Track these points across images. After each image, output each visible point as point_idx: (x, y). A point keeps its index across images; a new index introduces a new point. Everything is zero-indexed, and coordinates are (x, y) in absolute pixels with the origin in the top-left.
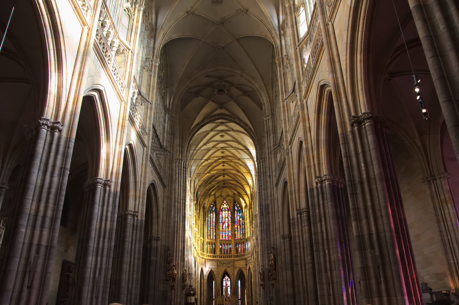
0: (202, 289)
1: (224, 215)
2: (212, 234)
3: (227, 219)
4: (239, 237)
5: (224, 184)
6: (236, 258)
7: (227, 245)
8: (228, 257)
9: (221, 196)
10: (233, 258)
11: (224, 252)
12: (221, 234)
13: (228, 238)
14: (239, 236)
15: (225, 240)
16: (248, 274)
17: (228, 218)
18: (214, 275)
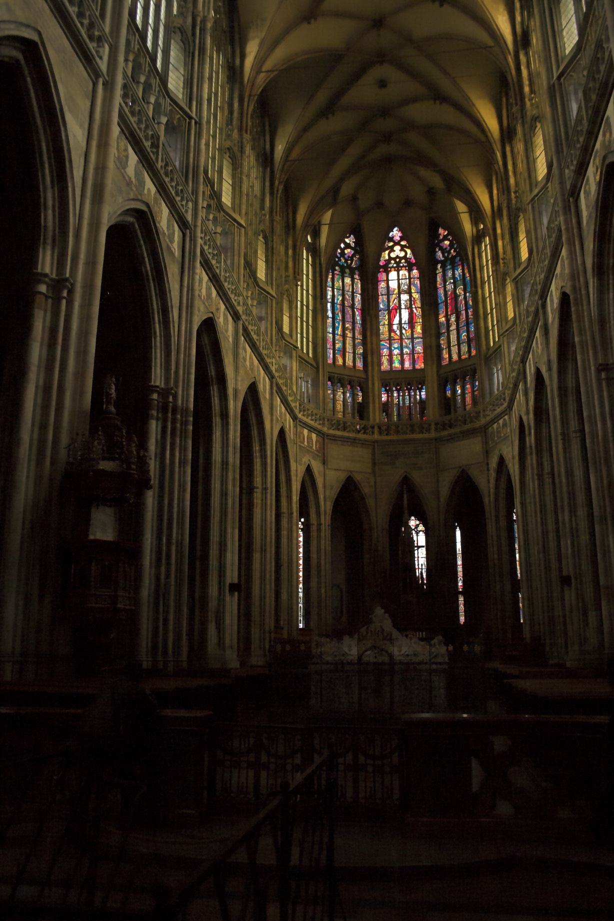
0: (314, 548)
1: (393, 285)
2: (349, 348)
3: (405, 297)
4: (455, 357)
5: (388, 138)
6: (445, 433)
7: (409, 390)
8: (413, 431)
9: (379, 205)
10: (433, 434)
11: (399, 415)
12: (385, 352)
13: (414, 362)
14: (454, 350)
15: (402, 369)
16: (497, 487)
17: (409, 292)
18: (363, 498)
